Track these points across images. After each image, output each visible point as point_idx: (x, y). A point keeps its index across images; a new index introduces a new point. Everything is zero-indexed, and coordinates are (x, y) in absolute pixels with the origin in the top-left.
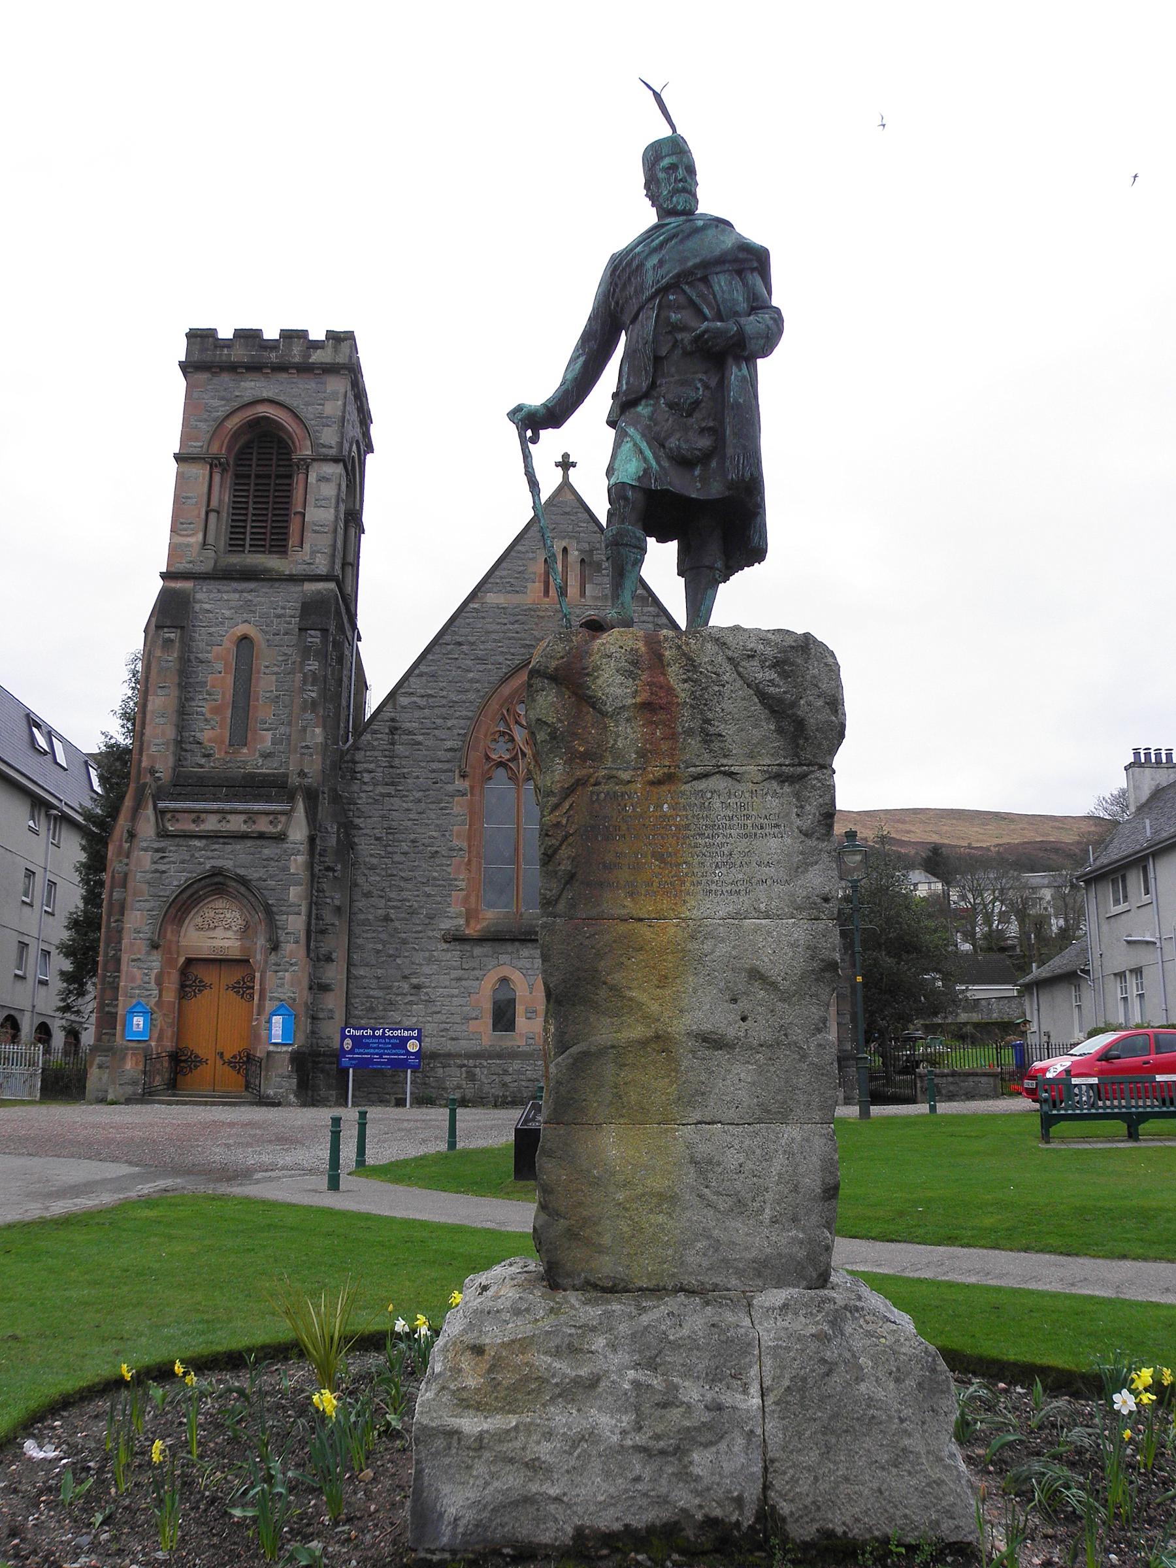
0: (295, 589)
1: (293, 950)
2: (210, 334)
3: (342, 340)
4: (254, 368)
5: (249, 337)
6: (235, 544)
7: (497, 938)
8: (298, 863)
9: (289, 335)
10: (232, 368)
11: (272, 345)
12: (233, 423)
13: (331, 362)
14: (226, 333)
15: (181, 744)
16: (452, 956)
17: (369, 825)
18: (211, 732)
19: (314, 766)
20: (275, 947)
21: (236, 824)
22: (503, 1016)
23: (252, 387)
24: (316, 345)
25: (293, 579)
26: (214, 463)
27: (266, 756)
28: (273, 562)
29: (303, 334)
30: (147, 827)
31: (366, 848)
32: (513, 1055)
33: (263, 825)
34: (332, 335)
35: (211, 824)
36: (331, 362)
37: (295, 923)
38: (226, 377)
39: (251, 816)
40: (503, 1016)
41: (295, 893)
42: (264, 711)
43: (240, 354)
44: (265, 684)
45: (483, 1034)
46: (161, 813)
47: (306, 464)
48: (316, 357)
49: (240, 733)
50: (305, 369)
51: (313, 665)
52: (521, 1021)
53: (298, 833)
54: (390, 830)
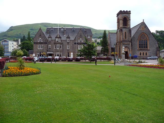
0: (128, 29)
1: (130, 51)
2: (122, 11)
3: (130, 11)
4: (125, 13)
5: (124, 11)
6: (124, 26)
7: (140, 50)
8: (131, 46)
9: (126, 11)
10: (123, 13)
11: (125, 12)
12: (124, 17)
13: (128, 13)
14: (122, 11)
15: (123, 39)
16: (138, 51)
17: (133, 43)
18: (124, 38)
19: (131, 40)
20: (129, 50)
21: (127, 44)
22: (140, 54)
23: (125, 15)
24: (128, 12)
25: (128, 28)
26: (123, 20)
27: (127, 39)
28: (126, 27)
29: (127, 11)
30: (122, 44)
31: (133, 45)
32: (141, 57)
33: (128, 44)
34: (129, 11)
35: (126, 44)
36: (128, 13)
37: (131, 49)
38: (123, 14)
39: (128, 43)
40: (140, 54)
41: (130, 48)
42: (127, 36)
43: (124, 12)
44: (127, 35)
45: (140, 56)
46: (123, 43)
47: (128, 20)
48: (128, 13)
49: (126, 38)
50: (128, 13)
51: (130, 34)
52: (141, 55)
53: (130, 44)
54: (134, 44)
